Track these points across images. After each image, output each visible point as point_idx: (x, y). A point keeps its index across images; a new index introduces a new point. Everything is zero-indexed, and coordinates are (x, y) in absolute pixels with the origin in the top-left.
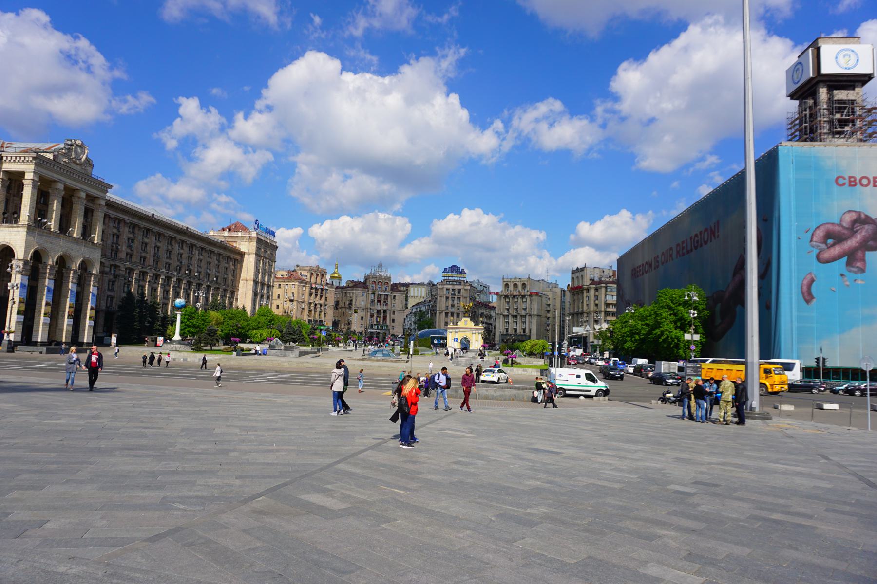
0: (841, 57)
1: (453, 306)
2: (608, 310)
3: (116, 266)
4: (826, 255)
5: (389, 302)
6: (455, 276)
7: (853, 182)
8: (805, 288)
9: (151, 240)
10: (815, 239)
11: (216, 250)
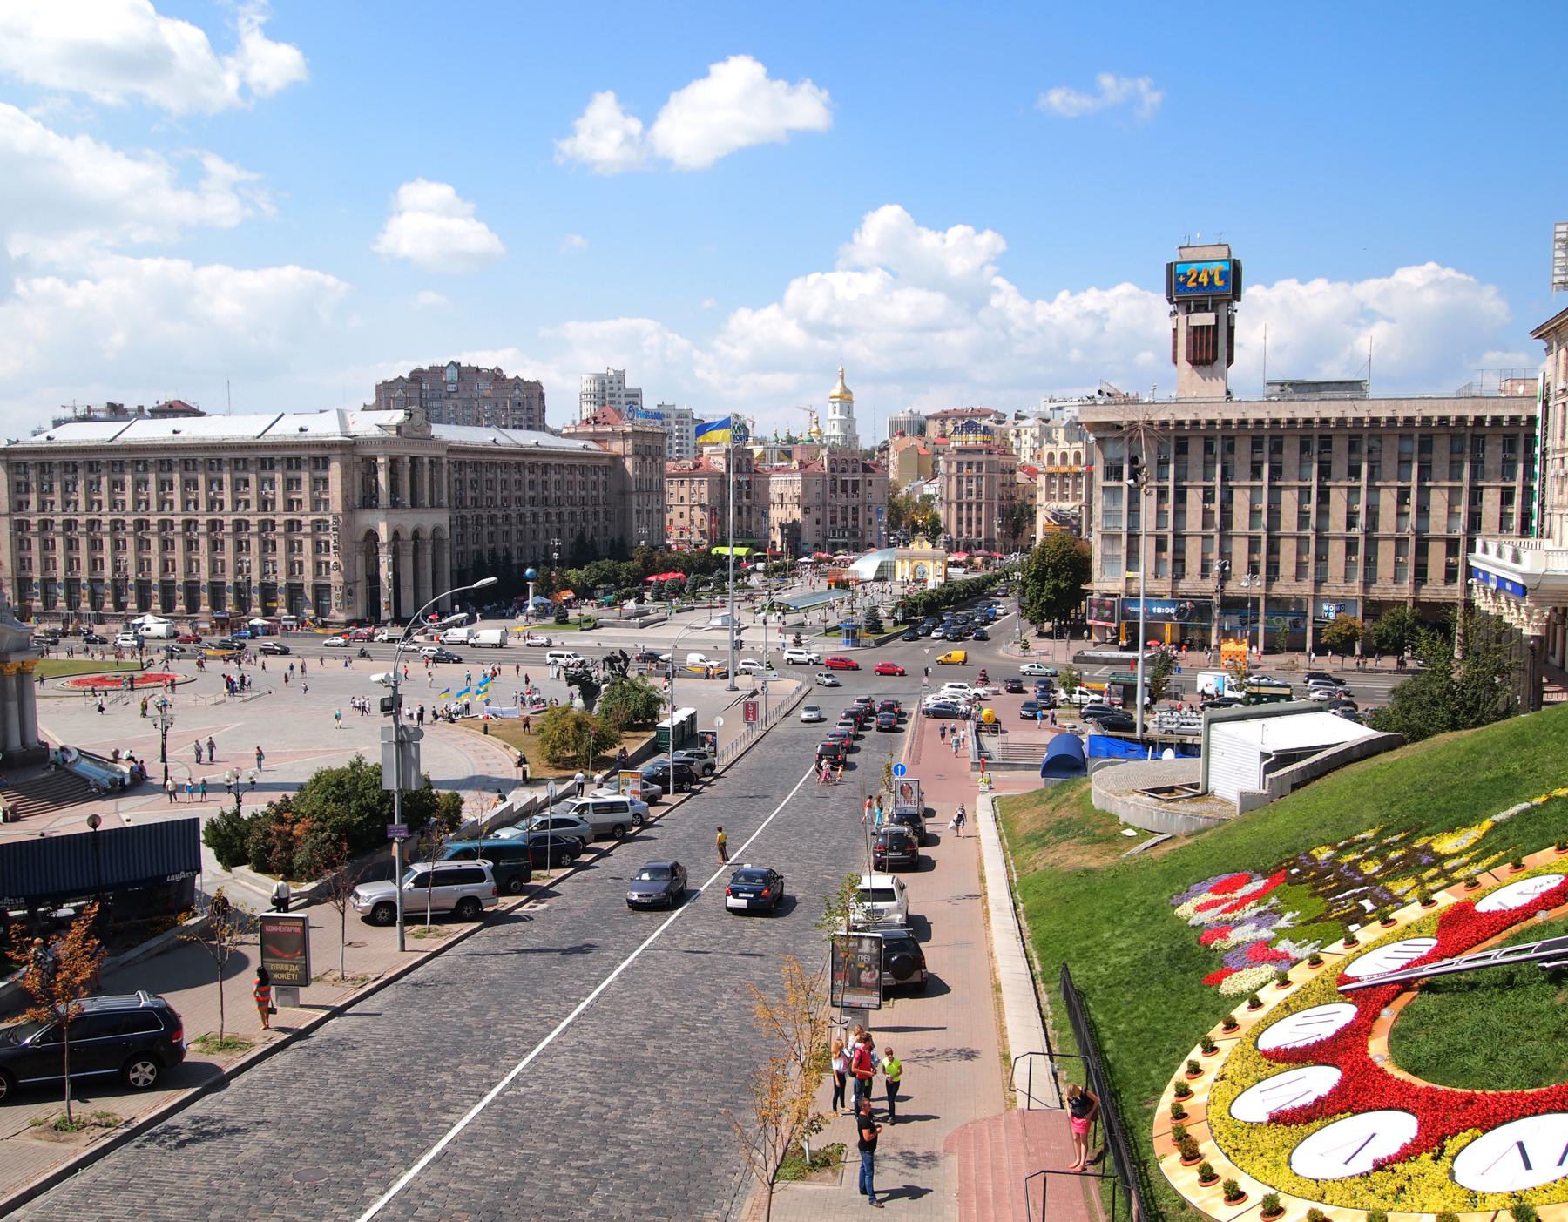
1: (970, 492)
3: (462, 517)
5: (860, 491)
9: (500, 475)
11: (577, 462)
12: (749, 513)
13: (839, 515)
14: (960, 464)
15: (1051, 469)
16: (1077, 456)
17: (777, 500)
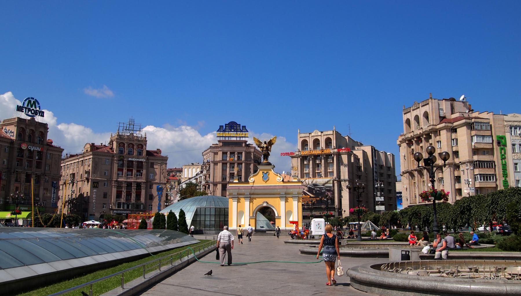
2: (476, 158)
6: (233, 136)
12: (37, 182)
13: (124, 190)
14: (224, 153)
15: (305, 153)
16: (328, 142)
17: (69, 179)
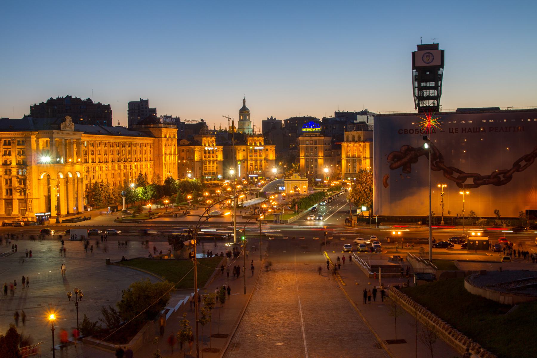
0: (425, 57)
4: (394, 166)
7: (406, 132)
8: (384, 181)
10: (389, 159)
